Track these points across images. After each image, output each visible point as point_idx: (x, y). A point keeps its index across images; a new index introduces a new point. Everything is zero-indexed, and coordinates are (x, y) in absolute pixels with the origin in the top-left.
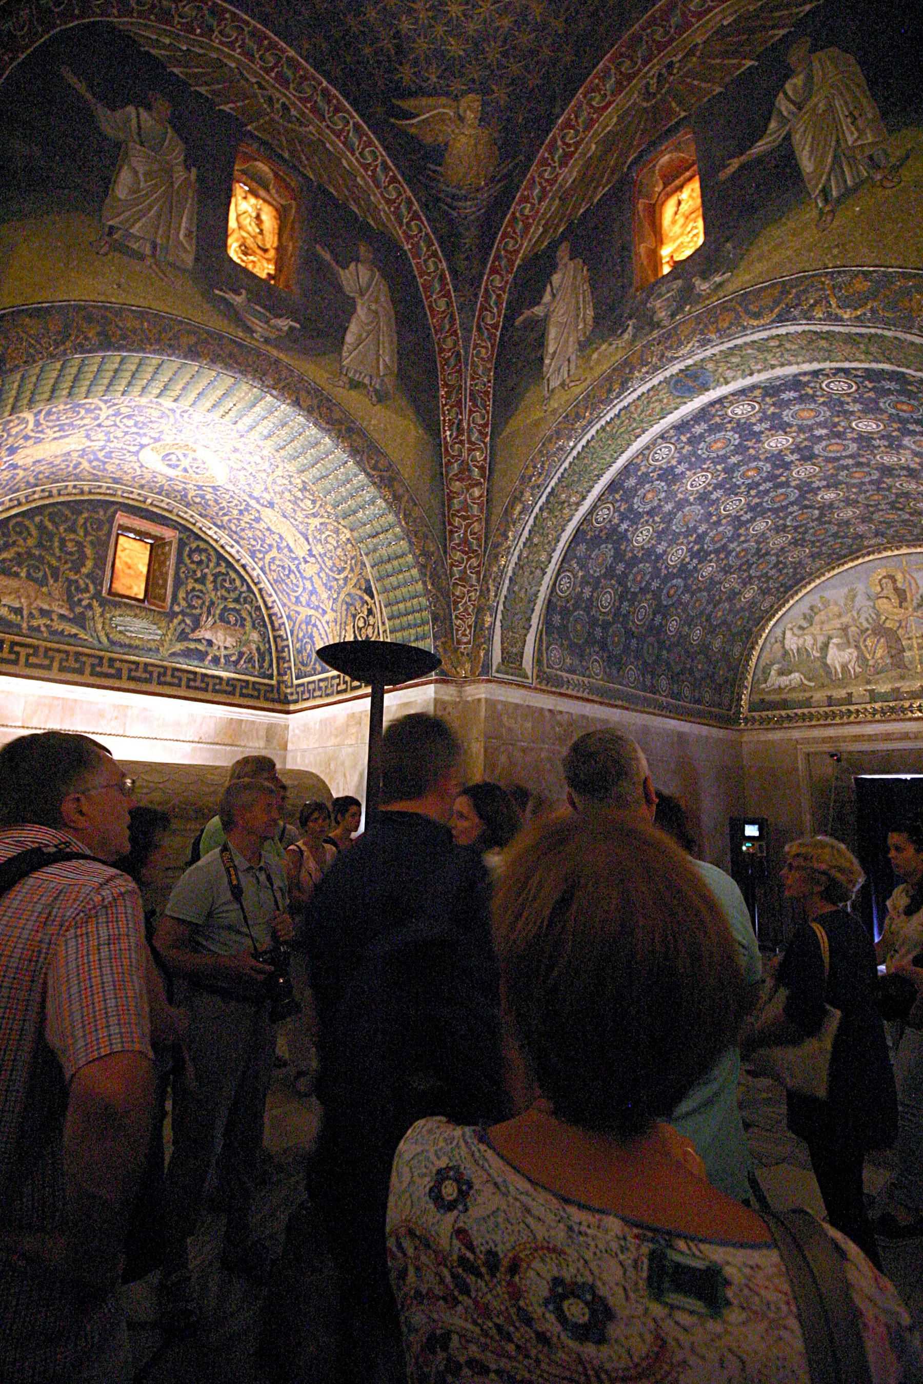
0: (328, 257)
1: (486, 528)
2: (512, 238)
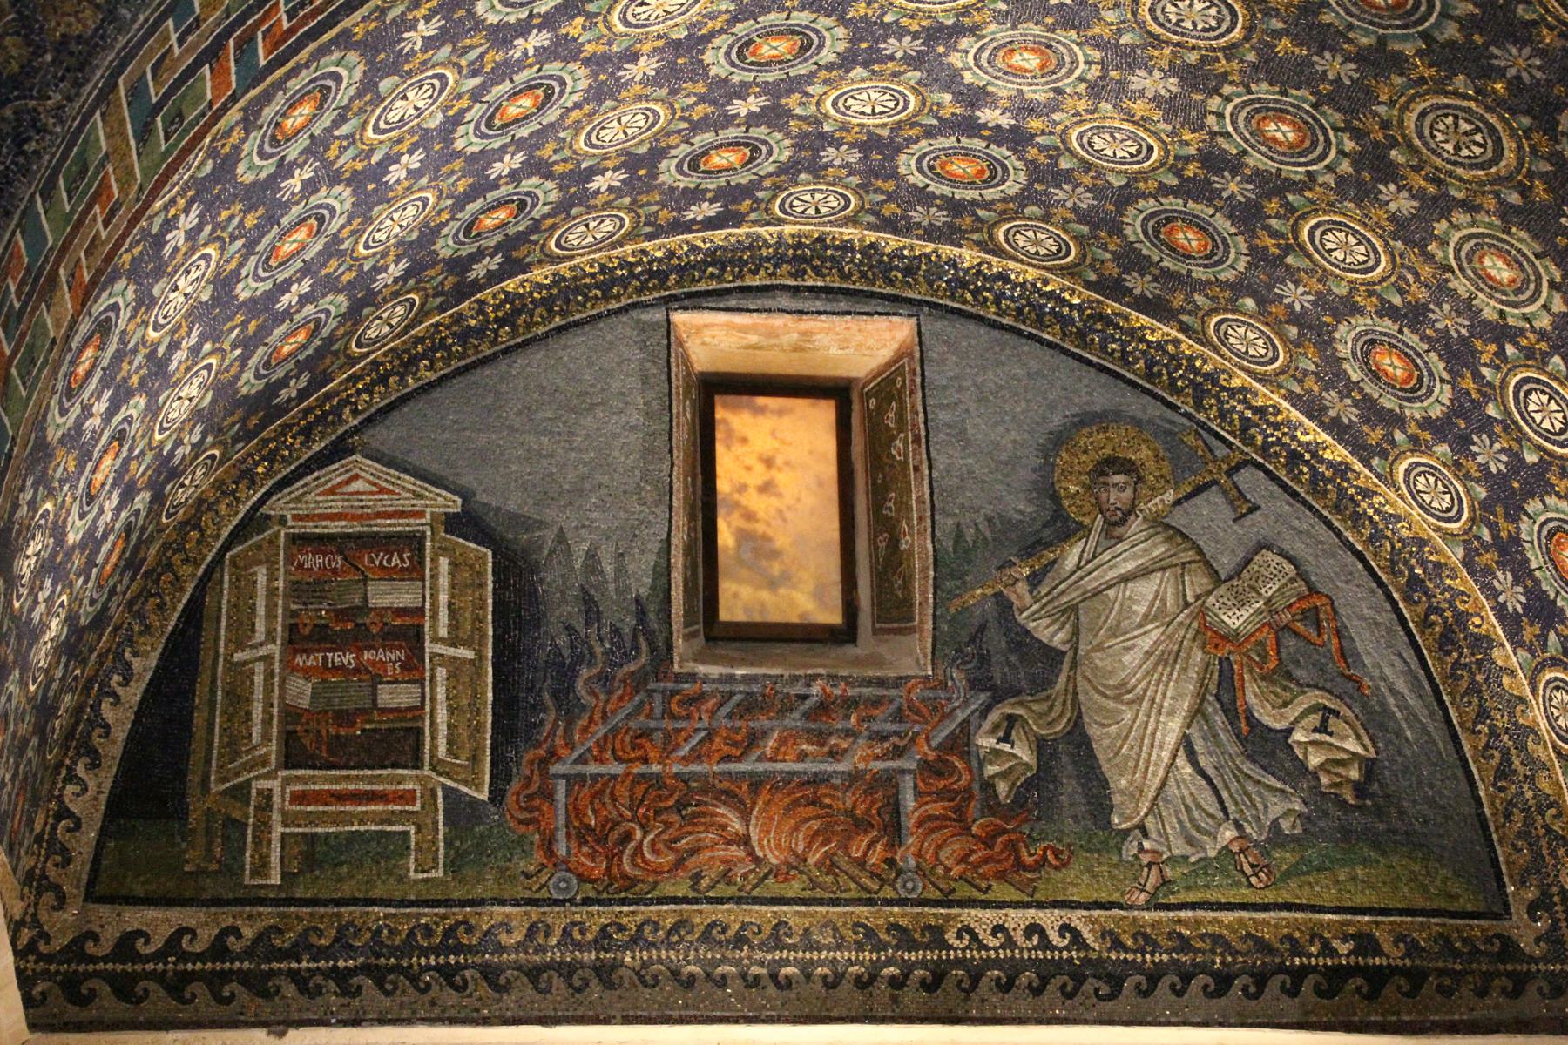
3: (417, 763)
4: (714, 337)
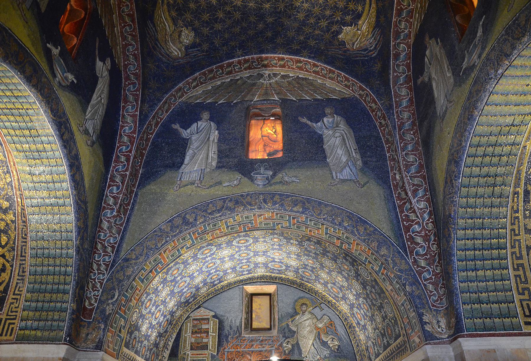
3: (207, 350)
4: (250, 289)
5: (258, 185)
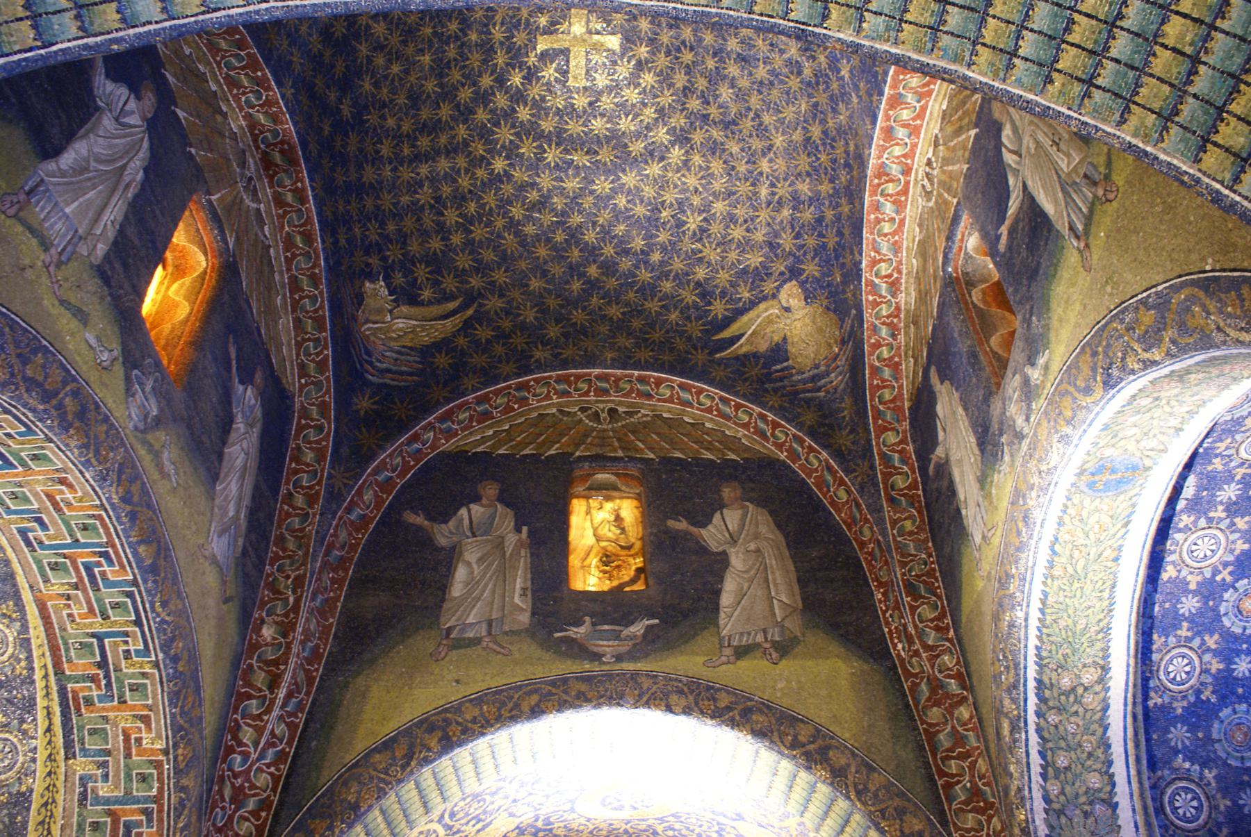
0: (682, 525)
1: (991, 765)
2: (884, 387)
5: (130, 416)
